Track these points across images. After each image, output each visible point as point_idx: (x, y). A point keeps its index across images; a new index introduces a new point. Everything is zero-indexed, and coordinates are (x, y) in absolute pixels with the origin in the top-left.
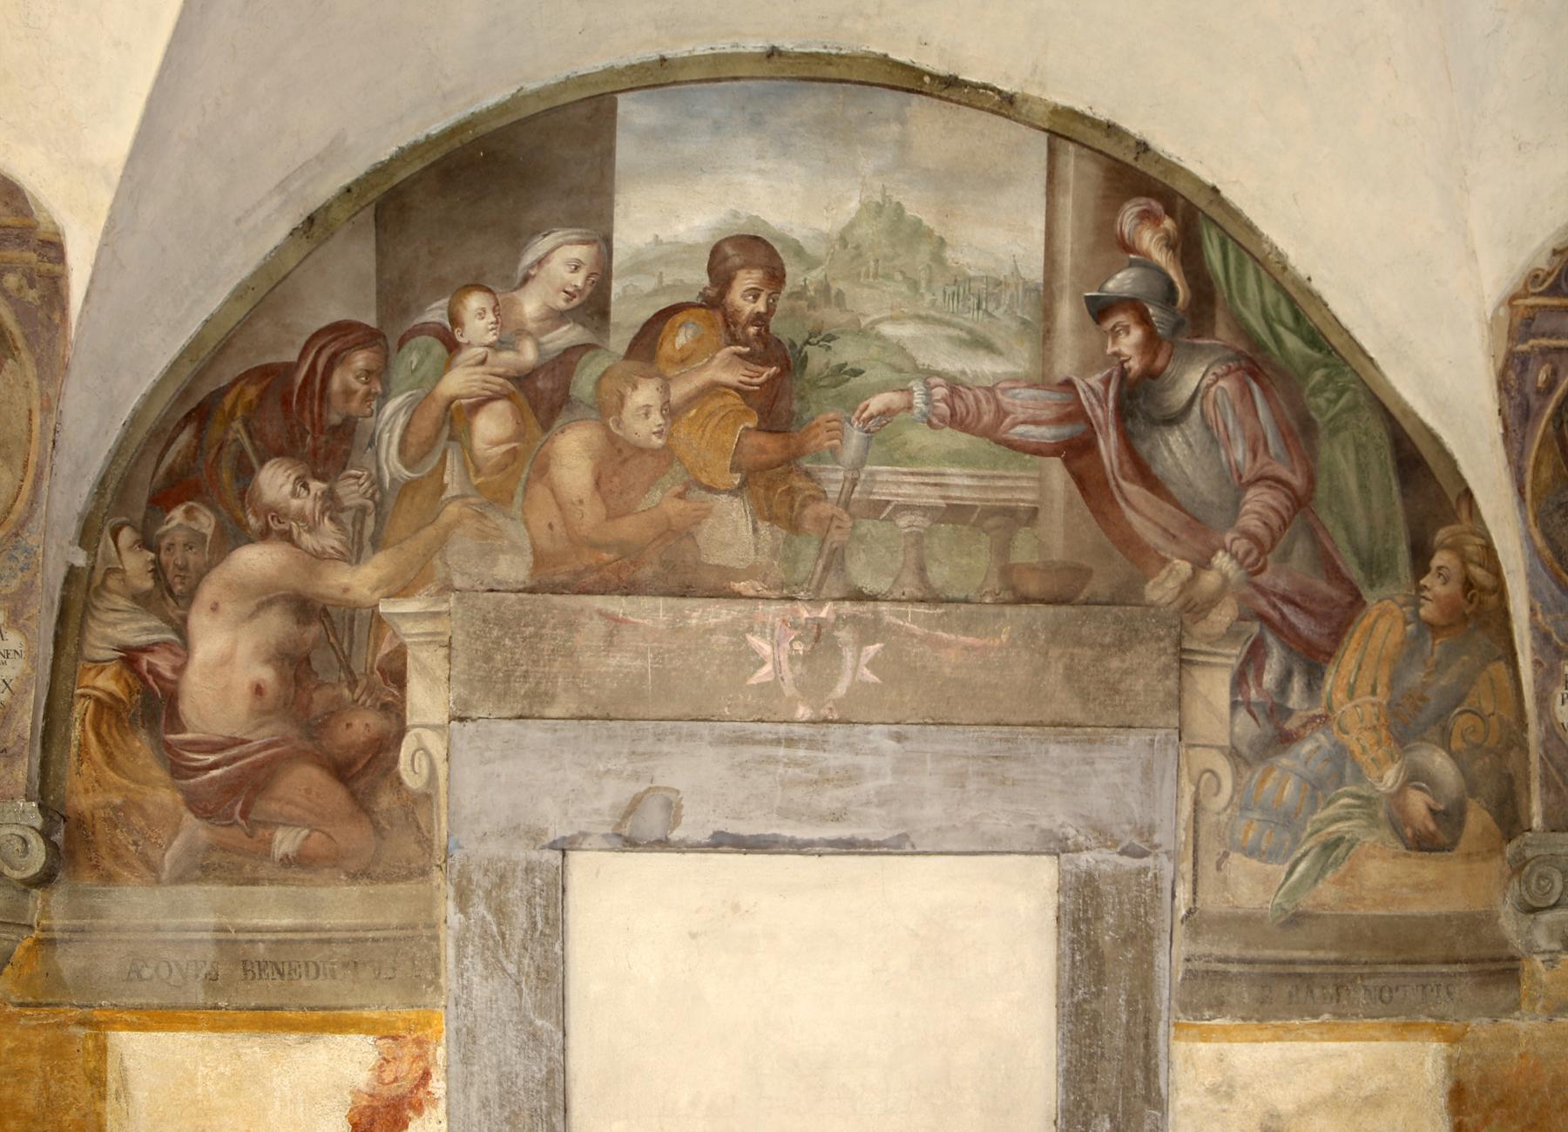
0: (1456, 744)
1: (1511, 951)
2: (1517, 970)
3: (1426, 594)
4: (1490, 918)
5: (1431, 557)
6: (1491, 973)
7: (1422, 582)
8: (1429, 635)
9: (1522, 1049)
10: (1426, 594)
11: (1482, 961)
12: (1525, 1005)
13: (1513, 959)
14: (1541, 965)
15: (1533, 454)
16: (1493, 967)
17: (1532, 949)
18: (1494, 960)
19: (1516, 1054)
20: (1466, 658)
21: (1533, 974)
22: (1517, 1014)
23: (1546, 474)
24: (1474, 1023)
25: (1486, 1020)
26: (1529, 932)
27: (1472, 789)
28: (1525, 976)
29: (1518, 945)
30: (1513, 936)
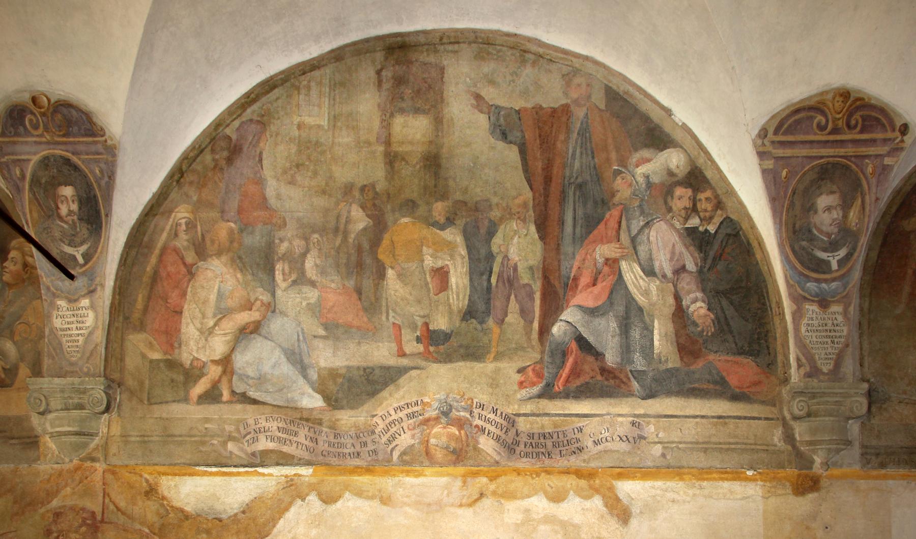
0: (17, 338)
1: (36, 433)
2: (38, 442)
3: (6, 270)
4: (27, 418)
5: (8, 253)
6: (27, 444)
7: (4, 265)
8: (7, 289)
9: (41, 479)
10: (6, 270)
11: (24, 438)
12: (42, 458)
13: (36, 437)
14: (49, 439)
15: (27, 207)
16: (28, 441)
17: (45, 432)
18: (29, 437)
19: (38, 481)
20: (23, 298)
21: (45, 443)
22: (39, 462)
23: (35, 215)
24: (21, 467)
25: (26, 465)
26: (44, 424)
27: (22, 359)
28: (41, 444)
29: (39, 430)
30: (37, 426)
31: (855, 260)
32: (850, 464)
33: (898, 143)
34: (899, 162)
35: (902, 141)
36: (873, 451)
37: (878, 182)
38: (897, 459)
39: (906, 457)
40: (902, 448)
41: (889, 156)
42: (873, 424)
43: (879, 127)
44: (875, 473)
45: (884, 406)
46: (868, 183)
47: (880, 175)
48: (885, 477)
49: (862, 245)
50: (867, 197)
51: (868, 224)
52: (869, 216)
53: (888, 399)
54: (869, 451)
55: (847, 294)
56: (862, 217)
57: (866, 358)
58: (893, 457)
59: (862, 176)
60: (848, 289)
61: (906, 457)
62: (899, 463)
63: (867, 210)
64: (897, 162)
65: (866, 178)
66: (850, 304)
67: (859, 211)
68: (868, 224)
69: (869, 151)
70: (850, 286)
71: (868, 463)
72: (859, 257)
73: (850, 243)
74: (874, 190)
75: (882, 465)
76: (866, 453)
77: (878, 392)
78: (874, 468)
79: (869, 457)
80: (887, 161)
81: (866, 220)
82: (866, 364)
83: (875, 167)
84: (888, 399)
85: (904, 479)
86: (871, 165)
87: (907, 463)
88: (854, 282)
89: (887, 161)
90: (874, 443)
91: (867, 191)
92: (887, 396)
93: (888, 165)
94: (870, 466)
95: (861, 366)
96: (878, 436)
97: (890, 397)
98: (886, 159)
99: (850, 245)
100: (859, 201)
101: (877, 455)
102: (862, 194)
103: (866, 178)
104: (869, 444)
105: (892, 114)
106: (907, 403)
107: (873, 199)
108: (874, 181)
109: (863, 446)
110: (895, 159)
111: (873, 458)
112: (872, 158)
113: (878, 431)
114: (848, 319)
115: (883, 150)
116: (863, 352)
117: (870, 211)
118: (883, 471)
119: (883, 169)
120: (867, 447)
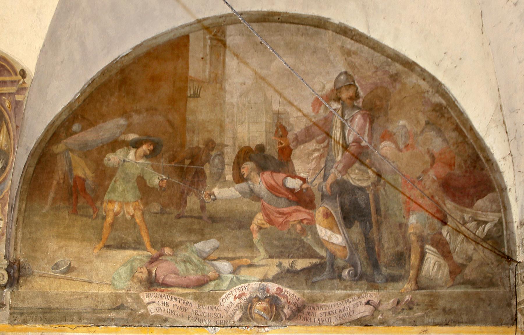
31: (8, 172)
32: (2, 321)
33: (22, 84)
34: (26, 98)
35: (24, 83)
36: (18, 311)
37: (15, 114)
38: (34, 317)
39: (41, 316)
40: (39, 309)
41: (18, 94)
42: (20, 292)
43: (6, 72)
44: (19, 327)
45: (29, 279)
46: (8, 114)
47: (15, 108)
48: (26, 330)
49: (12, 161)
50: (10, 125)
51: (14, 145)
52: (14, 139)
53: (32, 274)
54: (16, 311)
55: (3, 197)
56: (9, 140)
57: (19, 244)
58: (32, 316)
59: (3, 109)
60: (4, 193)
61: (41, 316)
62: (36, 320)
63: (12, 135)
64: (24, 98)
65: (6, 111)
66: (5, 205)
67: (6, 136)
68: (14, 145)
69: (3, 90)
70: (5, 191)
71: (15, 320)
72: (10, 170)
73: (3, 159)
74: (13, 120)
75: (25, 322)
76: (14, 313)
77: (25, 269)
78: (18, 324)
79: (15, 315)
80: (18, 98)
81: (12, 142)
82: (19, 249)
83: (10, 103)
84: (32, 274)
85: (39, 332)
86: (7, 101)
87: (41, 320)
88: (8, 188)
89: (18, 98)
90: (20, 305)
91: (9, 120)
92: (31, 272)
93: (19, 101)
94: (16, 322)
95: (15, 250)
96: (22, 301)
97: (33, 272)
98: (16, 96)
99: (4, 161)
100: (5, 127)
101: (22, 314)
102: (6, 123)
103: (6, 111)
104: (16, 306)
105: (12, 62)
106: (45, 277)
107: (15, 127)
108: (12, 113)
109: (11, 308)
110: (23, 96)
111: (19, 316)
112: (7, 95)
113: (23, 297)
114: (4, 215)
115: (12, 89)
116: (17, 240)
117: (14, 135)
118: (25, 326)
119: (16, 104)
120: (15, 308)
